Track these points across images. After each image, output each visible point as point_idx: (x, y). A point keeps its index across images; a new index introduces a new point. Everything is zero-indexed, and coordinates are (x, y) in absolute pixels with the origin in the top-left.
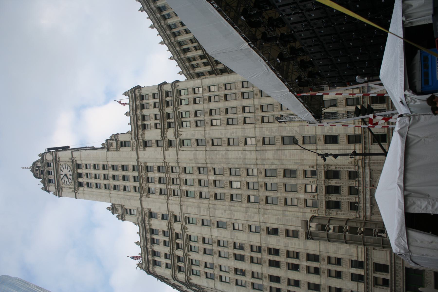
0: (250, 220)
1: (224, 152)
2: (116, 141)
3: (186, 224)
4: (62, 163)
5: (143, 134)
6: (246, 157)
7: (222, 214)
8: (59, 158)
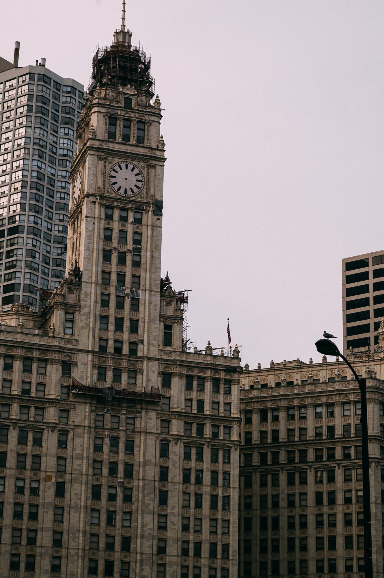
0: (71, 535)
1: (152, 509)
2: (175, 318)
3: (59, 431)
4: (145, 172)
5: (180, 375)
6: (145, 540)
7: (76, 494)
8: (153, 167)
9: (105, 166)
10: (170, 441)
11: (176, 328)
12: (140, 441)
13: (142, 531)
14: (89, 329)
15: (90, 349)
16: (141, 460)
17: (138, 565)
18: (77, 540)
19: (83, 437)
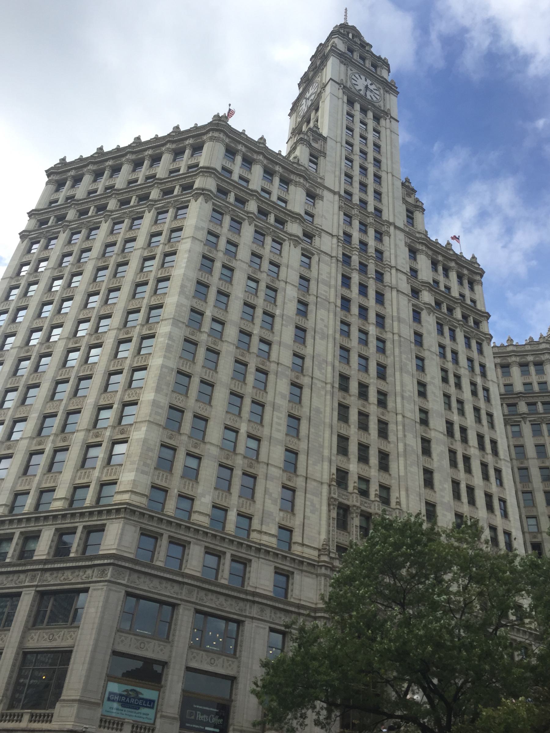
5: (427, 255)
7: (322, 320)
9: (347, 70)
10: (422, 310)
11: (417, 215)
12: (390, 296)
13: (403, 391)
14: (335, 176)
15: (336, 190)
16: (395, 314)
17: (400, 427)
18: (323, 371)
19: (330, 266)
